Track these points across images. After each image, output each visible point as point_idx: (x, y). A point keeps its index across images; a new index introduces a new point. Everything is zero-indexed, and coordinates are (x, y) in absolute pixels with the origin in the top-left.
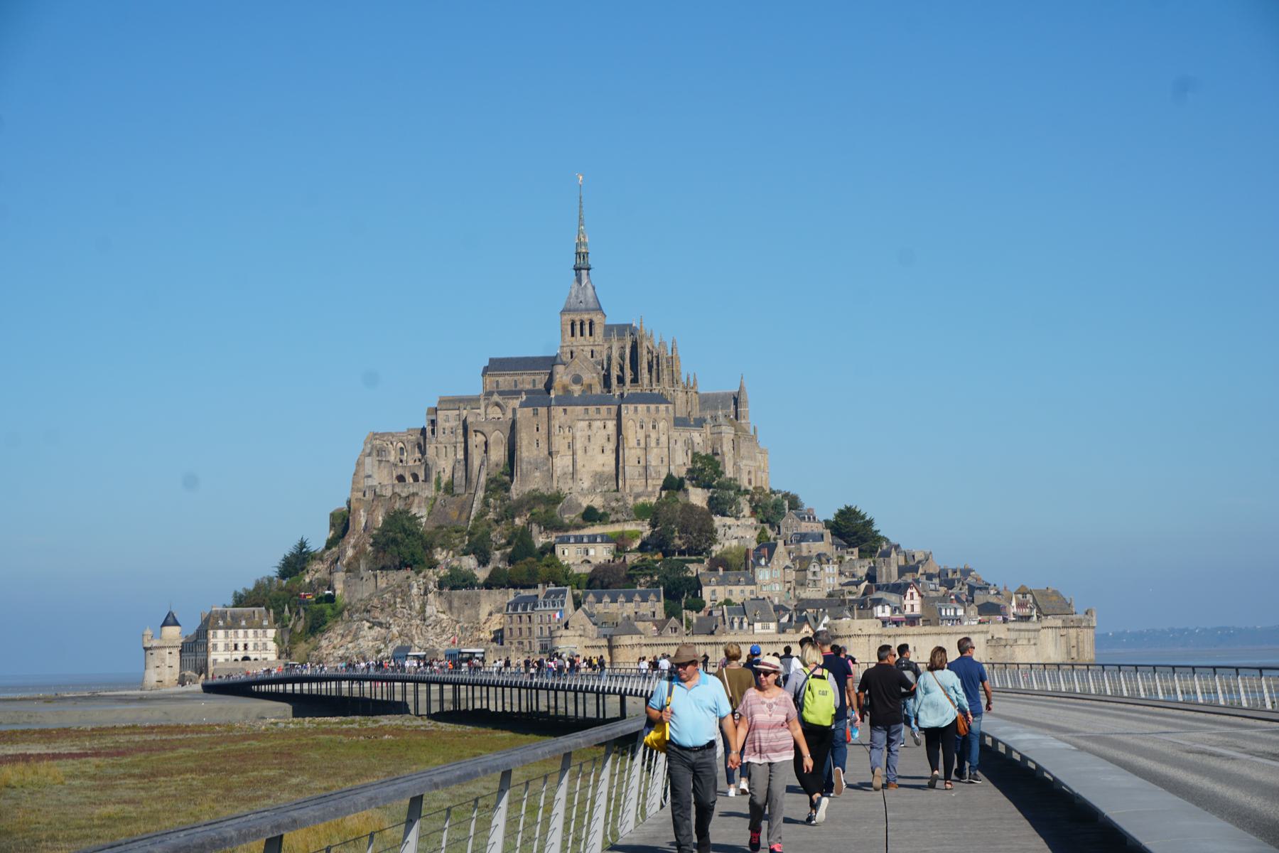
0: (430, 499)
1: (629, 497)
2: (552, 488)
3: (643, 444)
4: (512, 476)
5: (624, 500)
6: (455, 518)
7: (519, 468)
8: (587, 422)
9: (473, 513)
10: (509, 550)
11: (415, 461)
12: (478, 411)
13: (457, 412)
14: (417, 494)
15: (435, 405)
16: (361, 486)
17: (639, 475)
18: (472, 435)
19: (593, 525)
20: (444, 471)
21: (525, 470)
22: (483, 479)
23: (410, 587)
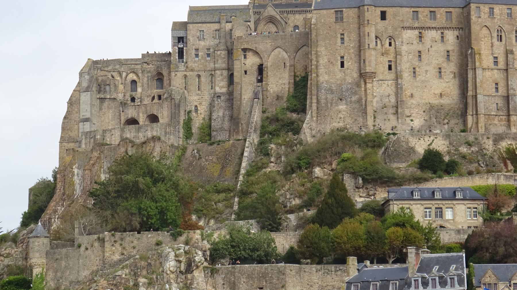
0: (177, 148)
1: (485, 140)
2: (366, 126)
3: (502, 64)
4: (303, 110)
5: (479, 144)
6: (216, 175)
7: (314, 98)
8: (416, 32)
9: (244, 164)
10: (311, 213)
11: (153, 98)
12: (249, 23)
13: (216, 26)
14: (159, 139)
15: (185, 19)
16: (73, 134)
17: (498, 110)
18: (238, 54)
19: (440, 177)
20: (196, 110)
21: (323, 101)
22: (257, 117)
23: (162, 257)
